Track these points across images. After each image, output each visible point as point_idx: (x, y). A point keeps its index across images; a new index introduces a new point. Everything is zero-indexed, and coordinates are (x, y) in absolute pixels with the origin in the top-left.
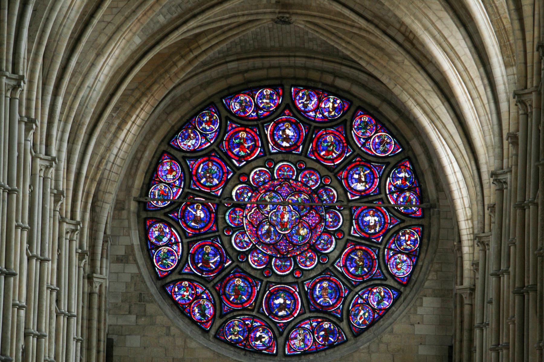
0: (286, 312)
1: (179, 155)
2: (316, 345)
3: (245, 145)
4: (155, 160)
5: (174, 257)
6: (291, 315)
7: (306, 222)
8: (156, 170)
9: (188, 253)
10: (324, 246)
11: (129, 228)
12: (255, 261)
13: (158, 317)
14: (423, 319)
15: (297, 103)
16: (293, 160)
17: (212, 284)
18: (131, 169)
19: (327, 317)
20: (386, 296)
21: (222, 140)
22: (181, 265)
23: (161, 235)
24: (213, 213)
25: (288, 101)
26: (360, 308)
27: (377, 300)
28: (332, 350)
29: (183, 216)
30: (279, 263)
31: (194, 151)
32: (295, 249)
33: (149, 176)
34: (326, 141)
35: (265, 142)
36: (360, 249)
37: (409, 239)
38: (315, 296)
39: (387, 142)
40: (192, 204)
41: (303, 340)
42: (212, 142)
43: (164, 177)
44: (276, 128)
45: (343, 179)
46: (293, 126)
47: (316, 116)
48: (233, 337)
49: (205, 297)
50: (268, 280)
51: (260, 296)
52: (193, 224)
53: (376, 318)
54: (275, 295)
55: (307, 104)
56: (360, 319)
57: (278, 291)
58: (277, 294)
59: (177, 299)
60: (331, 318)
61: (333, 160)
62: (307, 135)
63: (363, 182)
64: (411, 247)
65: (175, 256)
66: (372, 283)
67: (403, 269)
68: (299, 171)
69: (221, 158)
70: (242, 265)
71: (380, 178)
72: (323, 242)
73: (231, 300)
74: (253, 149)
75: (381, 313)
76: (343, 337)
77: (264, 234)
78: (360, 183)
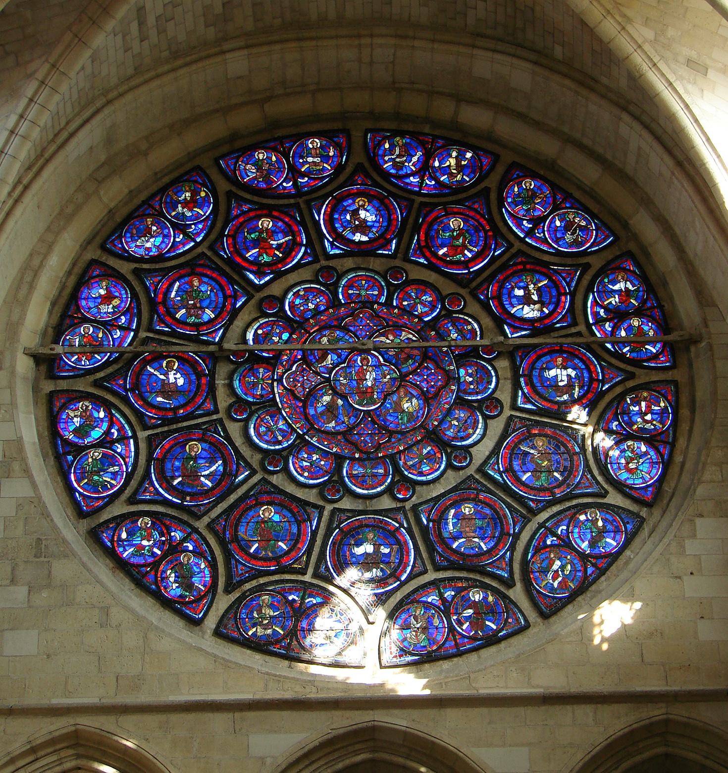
0: (382, 570)
1: (125, 268)
2: (455, 640)
3: (272, 242)
4: (72, 280)
5: (116, 468)
6: (395, 575)
7: (416, 385)
8: (74, 297)
9: (150, 459)
10: (459, 431)
11: (13, 404)
12: (303, 469)
13: (80, 587)
14: (700, 564)
15: (381, 161)
16: (378, 268)
17: (206, 520)
18: (18, 288)
19: (478, 577)
20: (609, 527)
21: (221, 235)
22: (134, 483)
23: (87, 425)
24: (205, 375)
25: (359, 157)
26: (552, 556)
27: (589, 536)
28: (493, 649)
29: (135, 387)
30: (358, 470)
31: (160, 258)
32: (393, 440)
33: (58, 311)
34: (446, 228)
35: (314, 236)
36: (540, 435)
37: (649, 410)
38: (446, 535)
39: (579, 226)
40: (156, 358)
41: (424, 629)
42: (198, 240)
43: (94, 310)
44: (337, 207)
45: (492, 298)
46: (375, 203)
47: (422, 183)
48: (260, 631)
49: (191, 548)
50: (336, 506)
51: (319, 542)
52: (160, 399)
53: (591, 575)
54: (353, 536)
55: (403, 163)
56: (554, 579)
57: (361, 526)
58: (358, 534)
59: (124, 556)
60: (487, 581)
61: (467, 264)
62: (405, 220)
63: (535, 303)
64: (654, 425)
65: (120, 465)
66: (574, 502)
67: (642, 471)
68: (392, 289)
69: (218, 269)
70: (275, 479)
71: (573, 295)
72: (457, 424)
73: (252, 551)
74: (289, 250)
75: (602, 563)
76: (517, 620)
77: (322, 413)
78: (529, 306)
